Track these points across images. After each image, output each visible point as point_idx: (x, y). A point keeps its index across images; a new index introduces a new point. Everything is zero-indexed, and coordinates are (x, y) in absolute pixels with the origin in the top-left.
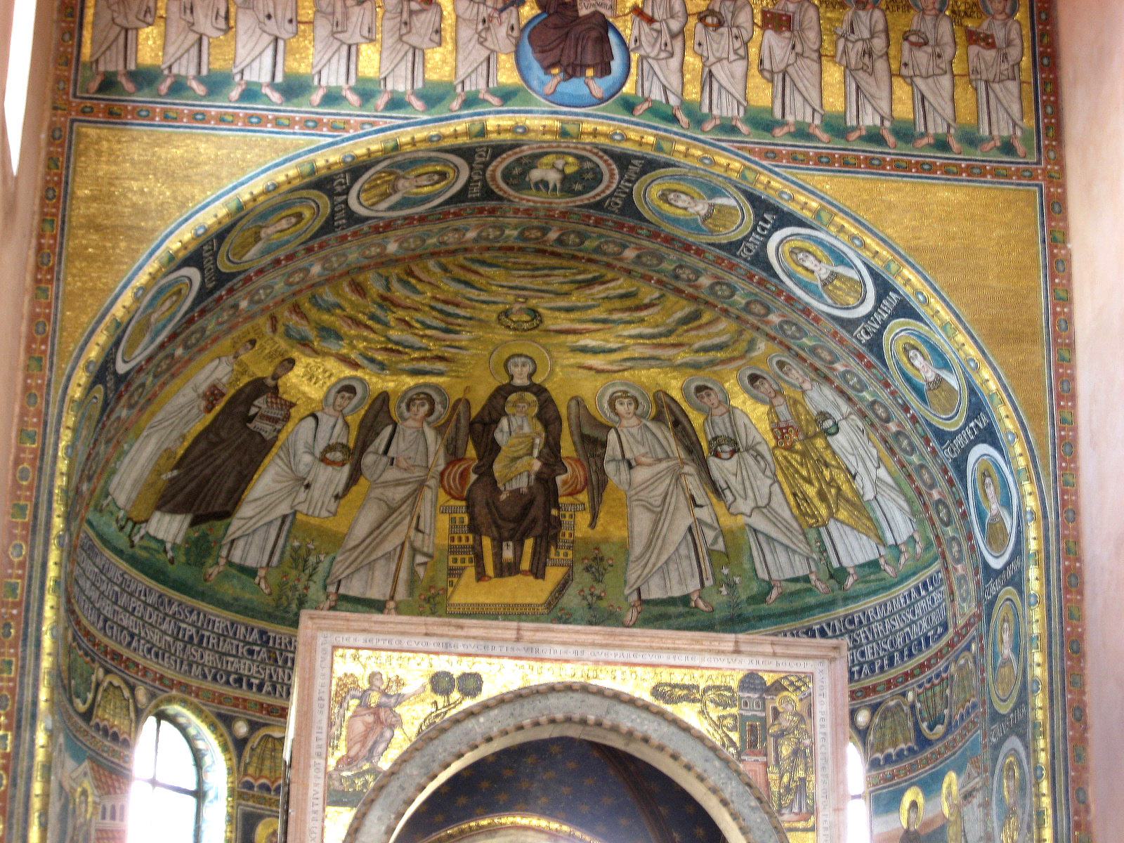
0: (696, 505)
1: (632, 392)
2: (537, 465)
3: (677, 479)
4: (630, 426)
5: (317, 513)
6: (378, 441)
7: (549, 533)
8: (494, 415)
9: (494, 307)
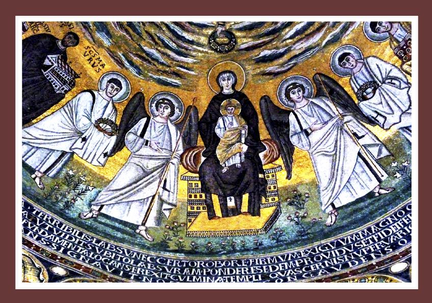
0: (359, 138)
1: (299, 82)
2: (245, 148)
3: (341, 129)
4: (302, 106)
5: (89, 160)
6: (136, 127)
7: (259, 190)
8: (213, 116)
9: (205, 31)
